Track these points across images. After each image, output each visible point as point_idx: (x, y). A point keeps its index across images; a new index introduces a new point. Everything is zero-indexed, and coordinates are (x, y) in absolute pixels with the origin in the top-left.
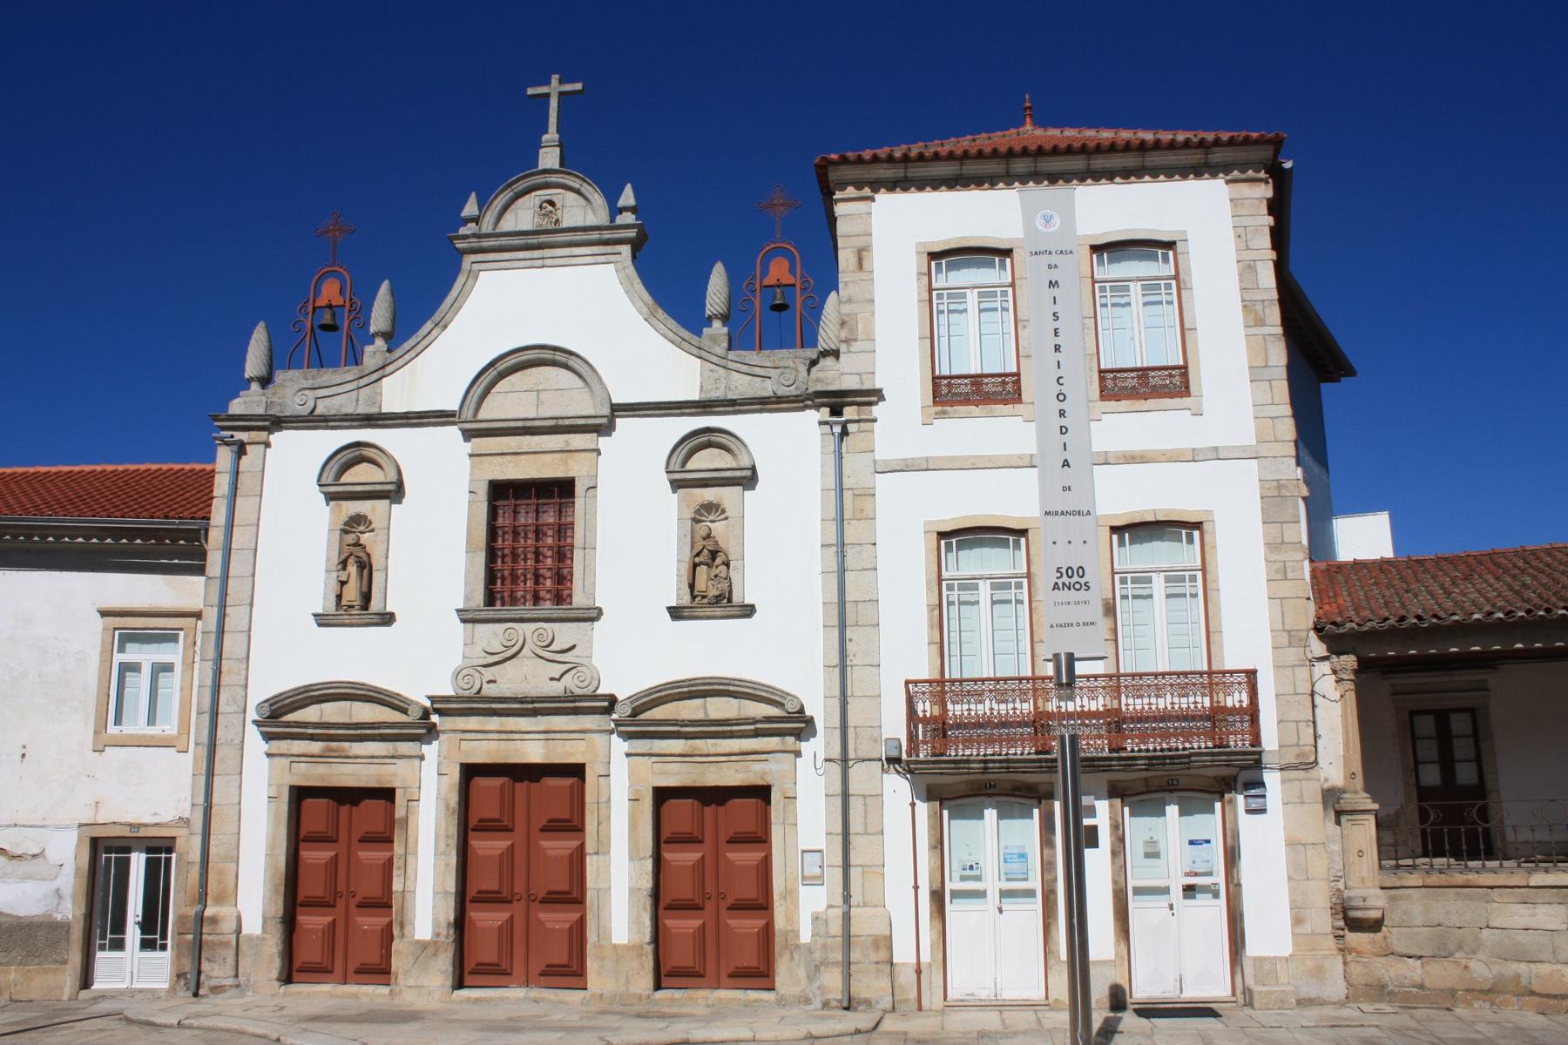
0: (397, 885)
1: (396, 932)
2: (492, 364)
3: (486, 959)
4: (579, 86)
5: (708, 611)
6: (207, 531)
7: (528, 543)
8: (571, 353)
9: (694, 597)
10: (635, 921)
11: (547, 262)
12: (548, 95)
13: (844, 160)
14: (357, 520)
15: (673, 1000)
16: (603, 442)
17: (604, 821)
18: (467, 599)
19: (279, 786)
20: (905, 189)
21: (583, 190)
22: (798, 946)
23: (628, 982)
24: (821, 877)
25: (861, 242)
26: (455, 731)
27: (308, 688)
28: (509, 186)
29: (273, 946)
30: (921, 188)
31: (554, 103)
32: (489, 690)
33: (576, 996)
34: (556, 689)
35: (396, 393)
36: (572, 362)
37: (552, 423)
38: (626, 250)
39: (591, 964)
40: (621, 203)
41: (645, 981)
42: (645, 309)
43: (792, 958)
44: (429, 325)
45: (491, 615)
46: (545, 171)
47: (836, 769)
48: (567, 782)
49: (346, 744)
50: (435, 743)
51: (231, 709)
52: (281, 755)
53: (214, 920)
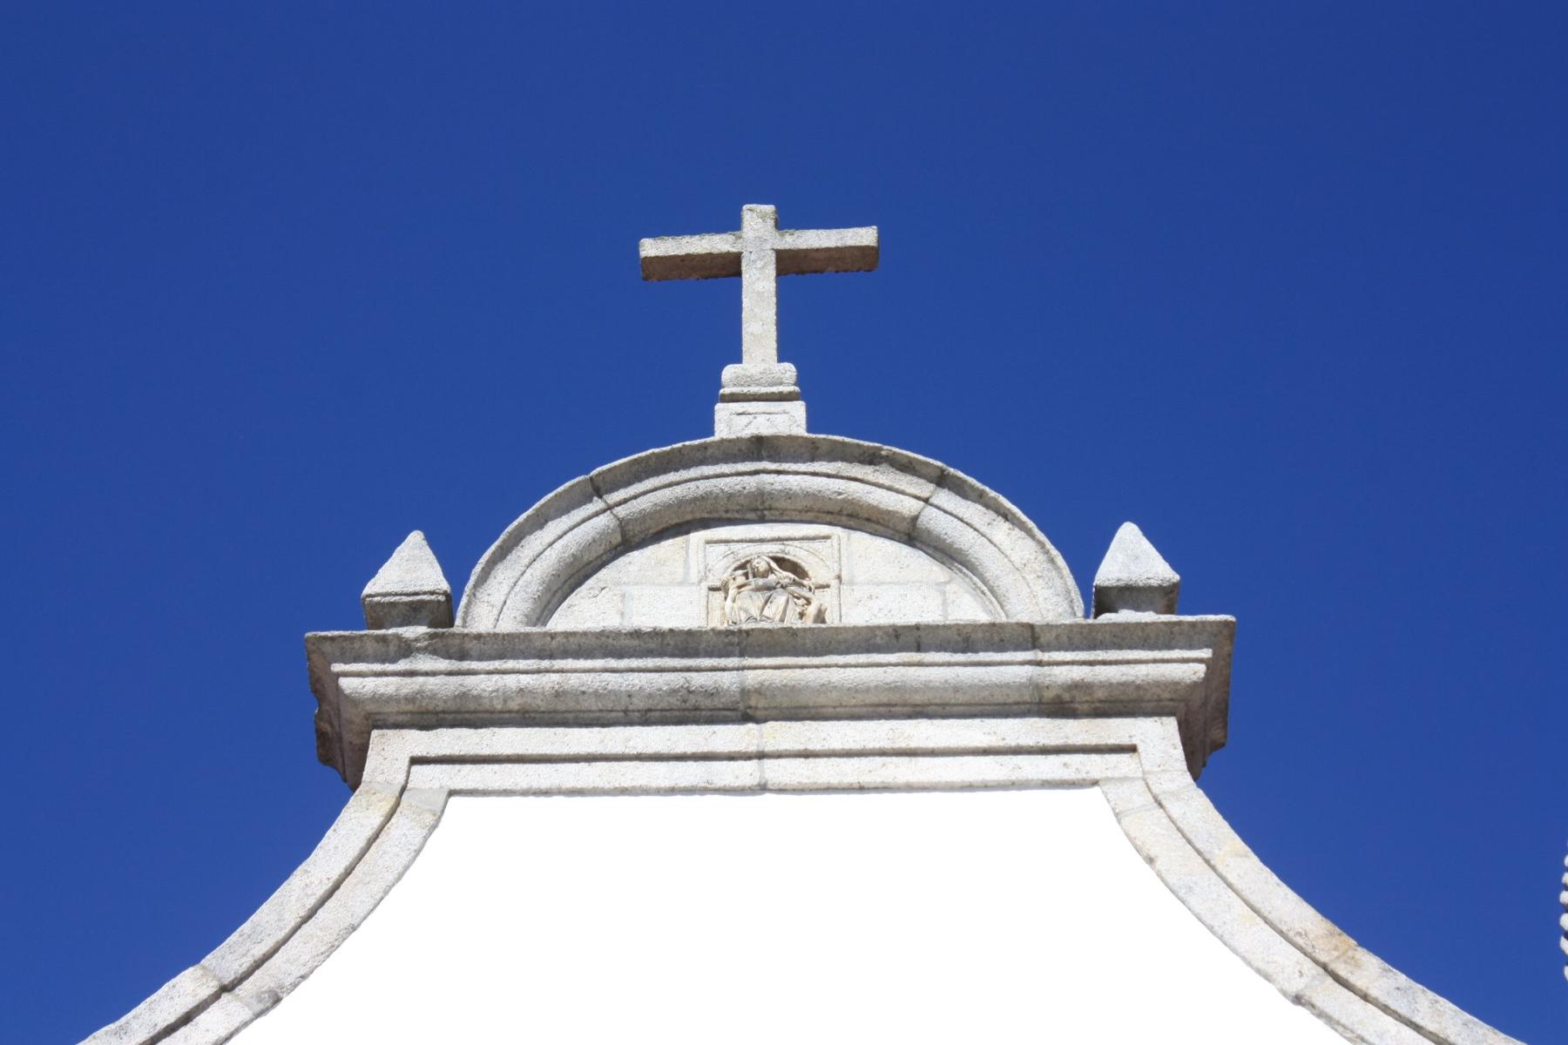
4: (865, 236)
11: (776, 771)
12: (730, 267)
21: (933, 520)
28: (597, 490)
38: (1159, 739)
40: (1110, 572)
42: (1287, 959)
44: (186, 987)
46: (760, 448)
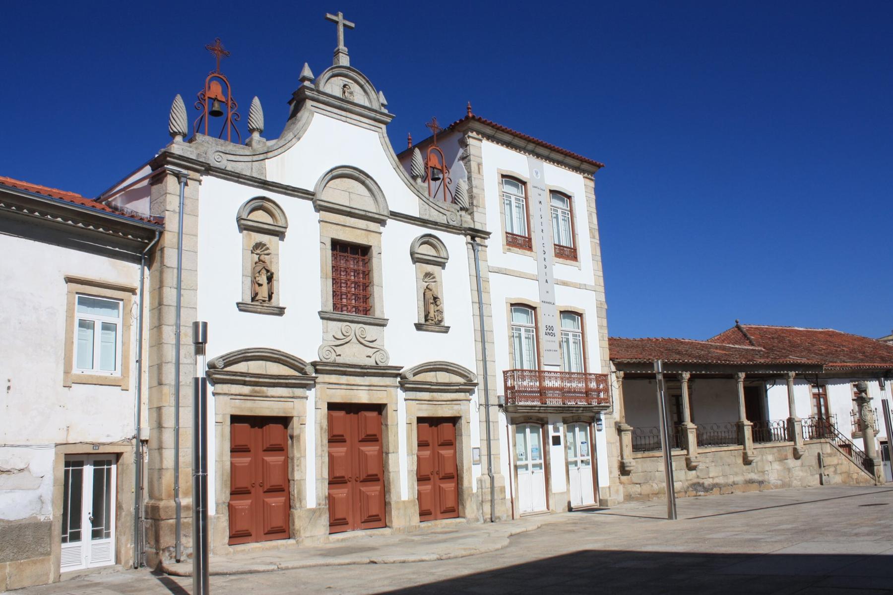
2: (331, 171)
3: (341, 517)
5: (433, 328)
6: (161, 233)
8: (368, 176)
9: (426, 320)
10: (411, 488)
11: (348, 120)
13: (479, 120)
14: (258, 245)
15: (429, 527)
16: (382, 229)
18: (324, 304)
19: (224, 415)
20: (493, 141)
24: (480, 460)
26: (325, 383)
27: (246, 351)
30: (498, 143)
31: (341, 29)
32: (339, 360)
33: (386, 531)
34: (371, 362)
35: (273, 170)
36: (368, 181)
37: (363, 213)
45: (338, 317)
47: (483, 409)
48: (374, 414)
49: (265, 389)
50: (313, 390)
51: (189, 361)
52: (225, 394)
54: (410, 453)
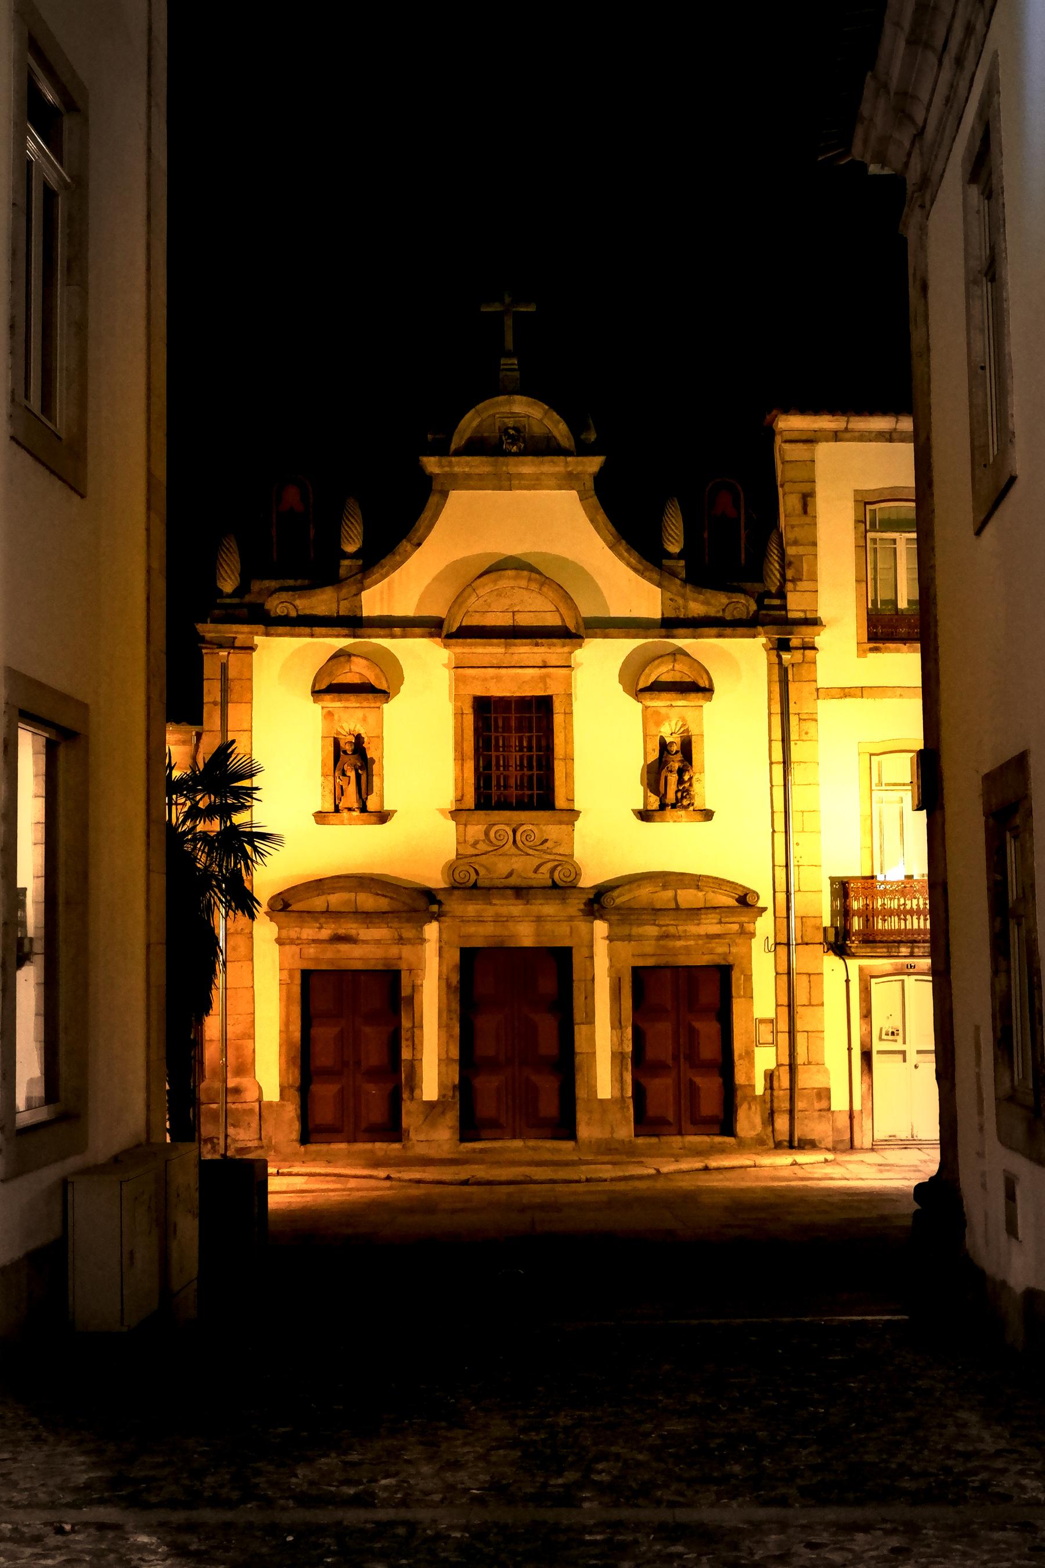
0: (406, 1054)
1: (405, 1095)
7: (514, 755)
10: (618, 1079)
17: (590, 996)
19: (291, 971)
22: (755, 1097)
23: (612, 1132)
25: (805, 488)
29: (291, 1110)
39: (581, 1117)
41: (625, 1131)
43: (750, 1108)
53: (237, 1091)
54: (617, 1023)
